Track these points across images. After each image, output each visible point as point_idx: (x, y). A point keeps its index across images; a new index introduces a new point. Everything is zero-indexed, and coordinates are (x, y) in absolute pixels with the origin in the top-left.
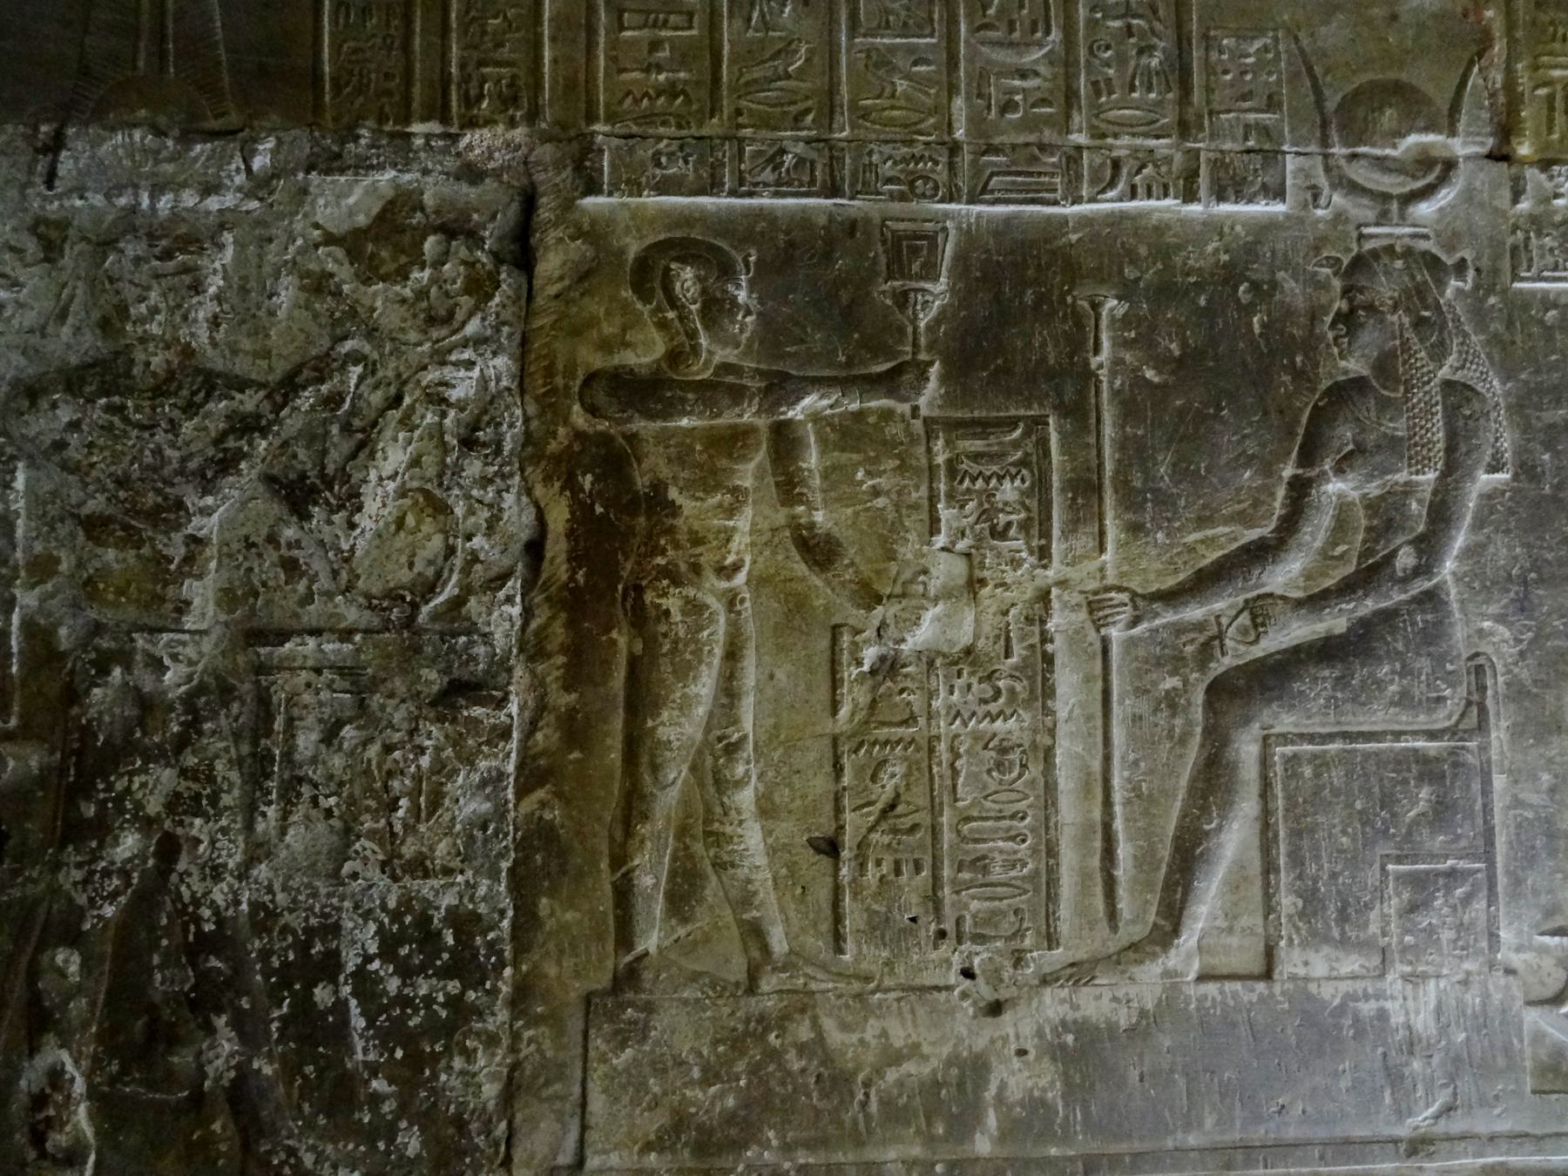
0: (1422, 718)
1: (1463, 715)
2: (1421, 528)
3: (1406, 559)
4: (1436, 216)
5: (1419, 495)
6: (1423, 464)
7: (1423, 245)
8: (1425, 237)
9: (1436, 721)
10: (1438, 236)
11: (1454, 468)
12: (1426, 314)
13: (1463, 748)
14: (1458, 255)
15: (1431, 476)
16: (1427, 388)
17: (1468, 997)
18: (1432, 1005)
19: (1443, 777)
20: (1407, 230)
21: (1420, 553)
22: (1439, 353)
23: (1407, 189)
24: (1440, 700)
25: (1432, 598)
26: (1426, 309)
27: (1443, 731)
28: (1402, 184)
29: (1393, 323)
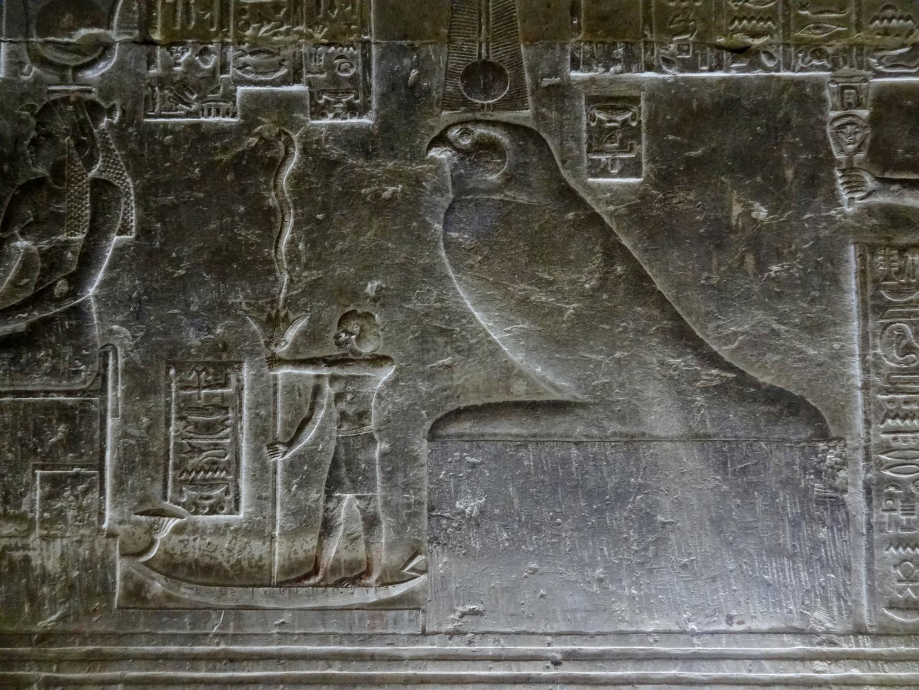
0: (64, 382)
1: (93, 382)
2: (74, 269)
3: (61, 287)
4: (100, 79)
5: (73, 249)
6: (75, 229)
7: (88, 96)
8: (90, 92)
9: (75, 384)
10: (100, 91)
11: (97, 233)
12: (85, 138)
13: (89, 401)
14: (112, 103)
15: (81, 237)
16: (81, 184)
17: (81, 550)
18: (58, 554)
19: (75, 418)
20: (76, 88)
21: (70, 283)
22: (90, 162)
23: (81, 62)
24: (77, 373)
25: (78, 313)
26: (85, 135)
27: (78, 391)
28: (76, 59)
29: (64, 144)
